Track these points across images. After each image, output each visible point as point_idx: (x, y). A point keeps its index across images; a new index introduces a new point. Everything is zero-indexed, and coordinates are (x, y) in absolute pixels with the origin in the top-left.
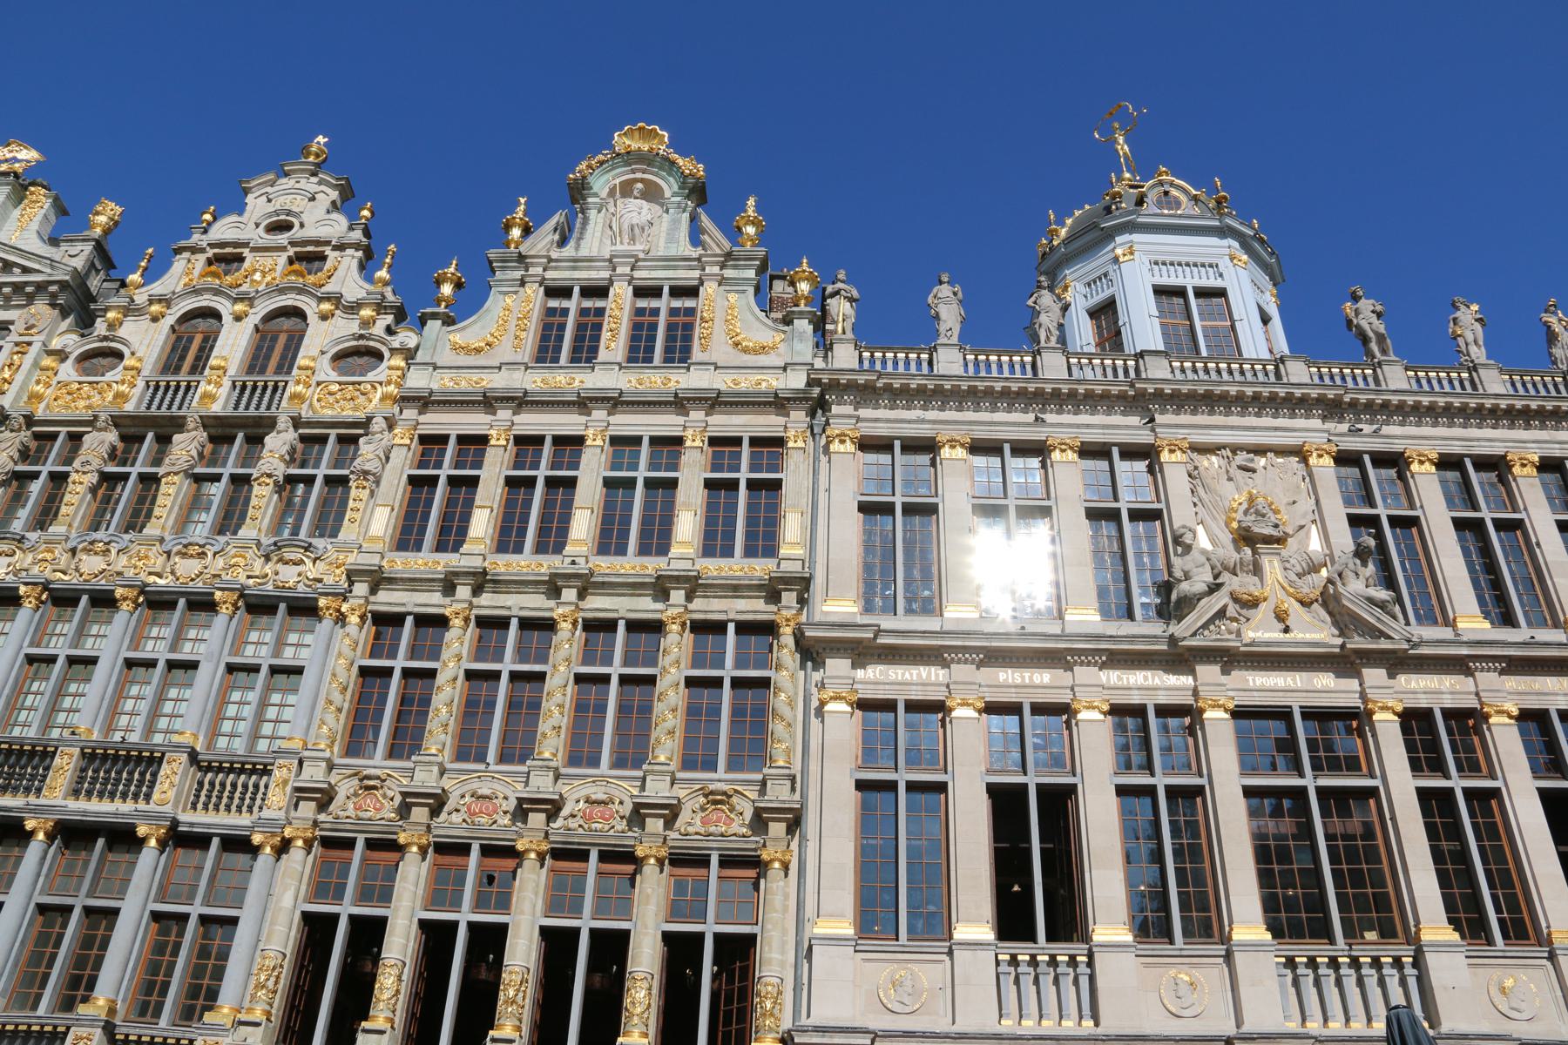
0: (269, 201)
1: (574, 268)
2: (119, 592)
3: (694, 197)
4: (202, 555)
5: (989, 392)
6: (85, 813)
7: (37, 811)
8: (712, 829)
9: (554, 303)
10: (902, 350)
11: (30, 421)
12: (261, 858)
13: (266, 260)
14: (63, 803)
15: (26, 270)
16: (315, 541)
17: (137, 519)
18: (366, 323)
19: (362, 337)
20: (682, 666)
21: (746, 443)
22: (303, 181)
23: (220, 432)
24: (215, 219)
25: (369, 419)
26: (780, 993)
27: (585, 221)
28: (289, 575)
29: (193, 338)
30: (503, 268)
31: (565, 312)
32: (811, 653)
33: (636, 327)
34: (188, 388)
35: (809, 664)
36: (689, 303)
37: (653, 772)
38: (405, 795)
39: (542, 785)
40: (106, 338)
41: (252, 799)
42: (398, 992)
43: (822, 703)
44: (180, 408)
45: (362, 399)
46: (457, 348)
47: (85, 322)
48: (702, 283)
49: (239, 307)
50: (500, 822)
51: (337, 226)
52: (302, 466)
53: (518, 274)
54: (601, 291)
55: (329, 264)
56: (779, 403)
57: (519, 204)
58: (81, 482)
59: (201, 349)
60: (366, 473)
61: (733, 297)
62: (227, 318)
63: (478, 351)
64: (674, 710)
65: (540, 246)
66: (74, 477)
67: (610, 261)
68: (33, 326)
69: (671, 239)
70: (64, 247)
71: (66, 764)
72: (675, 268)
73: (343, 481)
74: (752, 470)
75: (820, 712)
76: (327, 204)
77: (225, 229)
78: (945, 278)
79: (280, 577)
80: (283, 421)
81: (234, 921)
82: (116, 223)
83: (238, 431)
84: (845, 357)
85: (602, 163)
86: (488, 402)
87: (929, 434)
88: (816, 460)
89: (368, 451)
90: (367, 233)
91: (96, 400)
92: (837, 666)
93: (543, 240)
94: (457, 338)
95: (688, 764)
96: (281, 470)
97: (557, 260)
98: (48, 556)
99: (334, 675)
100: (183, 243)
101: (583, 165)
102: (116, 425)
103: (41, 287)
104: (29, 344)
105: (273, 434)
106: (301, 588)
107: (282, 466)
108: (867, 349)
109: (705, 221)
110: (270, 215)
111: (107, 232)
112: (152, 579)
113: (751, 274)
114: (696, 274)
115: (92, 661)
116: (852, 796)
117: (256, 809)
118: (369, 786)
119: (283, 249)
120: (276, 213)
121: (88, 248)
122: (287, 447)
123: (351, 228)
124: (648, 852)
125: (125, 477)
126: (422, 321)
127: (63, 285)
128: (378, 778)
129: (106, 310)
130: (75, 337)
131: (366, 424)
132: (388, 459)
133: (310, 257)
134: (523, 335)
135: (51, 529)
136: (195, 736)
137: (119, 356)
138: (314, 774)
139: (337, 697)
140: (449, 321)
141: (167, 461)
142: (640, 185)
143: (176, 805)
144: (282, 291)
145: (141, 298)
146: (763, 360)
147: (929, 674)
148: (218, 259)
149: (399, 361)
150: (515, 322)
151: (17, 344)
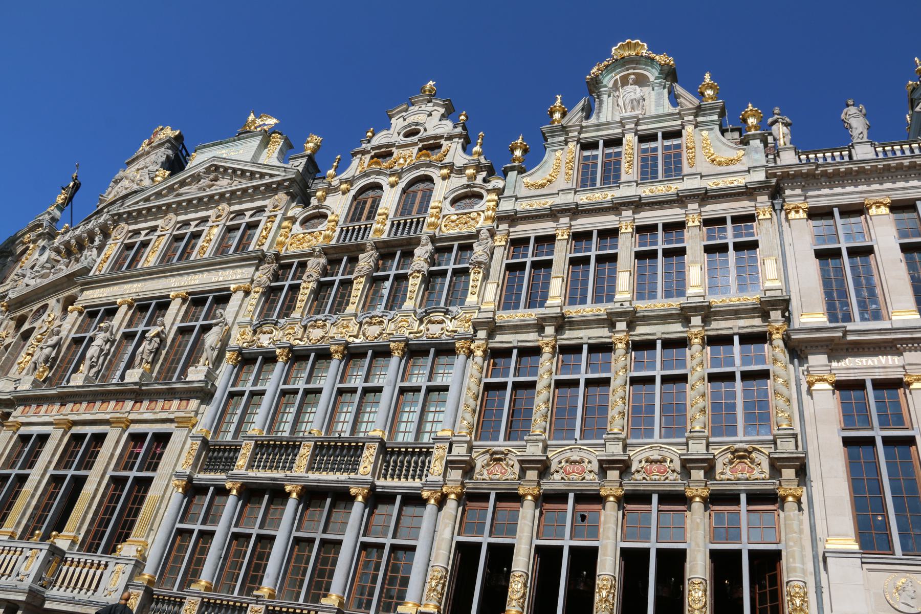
0: (405, 120)
1: (598, 130)
2: (333, 348)
3: (669, 78)
4: (381, 322)
5: (900, 167)
6: (319, 481)
7: (292, 480)
8: (740, 476)
9: (587, 153)
10: (828, 151)
11: (277, 257)
12: (429, 507)
13: (406, 152)
14: (306, 475)
15: (271, 176)
16: (450, 308)
17: (340, 305)
19: (468, 186)
20: (705, 366)
21: (729, 221)
23: (386, 251)
24: (374, 135)
25: (478, 232)
26: (805, 593)
27: (601, 102)
28: (435, 329)
29: (365, 201)
30: (552, 136)
31: (596, 157)
32: (797, 351)
33: (644, 160)
34: (366, 228)
35: (796, 361)
36: (676, 142)
37: (692, 438)
38: (521, 462)
39: (614, 450)
40: (317, 207)
41: (421, 470)
42: (524, 594)
43: (810, 384)
44: (362, 238)
45: (472, 222)
47: (306, 203)
48: (683, 128)
49: (393, 179)
50: (587, 477)
51: (447, 127)
52: (439, 265)
53: (562, 138)
54: (616, 142)
55: (444, 149)
56: (749, 192)
58: (307, 287)
59: (372, 207)
60: (480, 263)
61: (705, 133)
62: (386, 187)
63: (543, 186)
64: (703, 395)
65: (574, 120)
66: (303, 285)
67: (621, 122)
68: (277, 206)
69: (658, 104)
70: (291, 162)
71: (305, 451)
72: (664, 121)
73: (465, 272)
74: (735, 236)
75: (810, 392)
77: (380, 139)
78: (850, 102)
79: (430, 331)
80: (424, 238)
81: (413, 549)
82: (319, 147)
83: (397, 249)
84: (788, 158)
85: (607, 66)
87: (858, 201)
88: (780, 225)
89: (479, 251)
90: (464, 128)
91: (314, 242)
92: (817, 360)
93: (575, 116)
94: (527, 180)
95: (716, 431)
96: (425, 267)
97: (586, 127)
98: (290, 331)
99: (469, 389)
100: (357, 149)
101: (595, 70)
102: (325, 254)
103: (280, 184)
104: (275, 216)
106: (444, 337)
107: (426, 266)
108: (803, 153)
109: (679, 89)
110: (405, 127)
111: (315, 150)
112: (351, 339)
113: (715, 117)
114: (679, 122)
115: (319, 391)
116: (839, 449)
117: (424, 477)
118: (497, 458)
119: (416, 144)
120: (409, 125)
122: (428, 254)
123: (455, 127)
124: (695, 493)
125: (332, 283)
126: (505, 174)
128: (502, 453)
129: (315, 192)
130: (300, 209)
131: (476, 236)
132: (492, 254)
134: (571, 172)
135: (292, 316)
136: (383, 432)
137: (325, 216)
138: (460, 451)
139: (472, 403)
140: (521, 171)
141: (356, 270)
142: (633, 77)
143: (373, 474)
144: (417, 167)
145: (335, 182)
146: (732, 168)
147: (887, 360)
148: (377, 156)
149: (494, 196)
150: (564, 165)
151: (269, 217)
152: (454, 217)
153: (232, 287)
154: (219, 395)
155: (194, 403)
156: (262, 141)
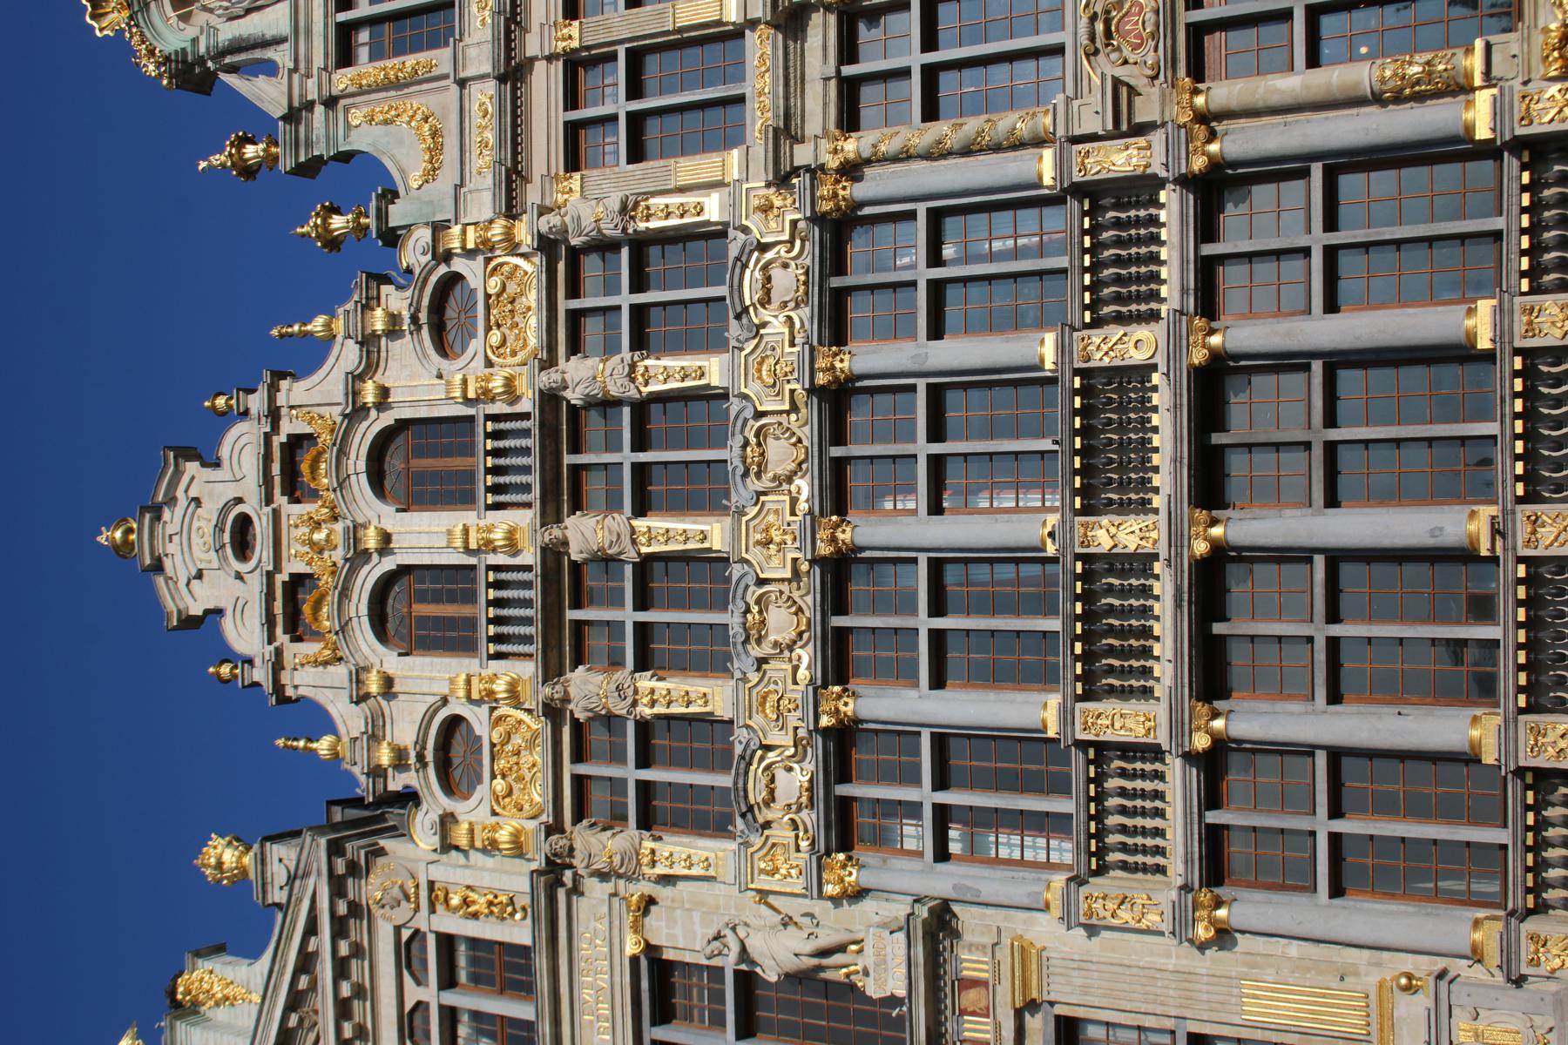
0: (199, 575)
15: (312, 929)
18: (394, 319)
22: (170, 529)
30: (309, 144)
45: (512, 288)
46: (432, 173)
51: (242, 446)
53: (319, 110)
57: (211, 167)
60: (624, 209)
63: (435, 133)
76: (208, 473)
77: (245, 634)
80: (548, 379)
82: (238, 840)
86: (513, 73)
93: (269, 94)
97: (296, 61)
100: (268, 687)
102: (561, 673)
103: (338, 888)
104: (431, 884)
105: (568, 394)
112: (803, 506)
119: (276, 514)
121: (276, 851)
127: (335, 849)
128: (1093, 18)
131: (547, 245)
133: (291, 467)
151: (432, 910)
152: (495, 338)
153: (632, 947)
154: (941, 881)
155: (970, 961)
156: (193, 1024)
